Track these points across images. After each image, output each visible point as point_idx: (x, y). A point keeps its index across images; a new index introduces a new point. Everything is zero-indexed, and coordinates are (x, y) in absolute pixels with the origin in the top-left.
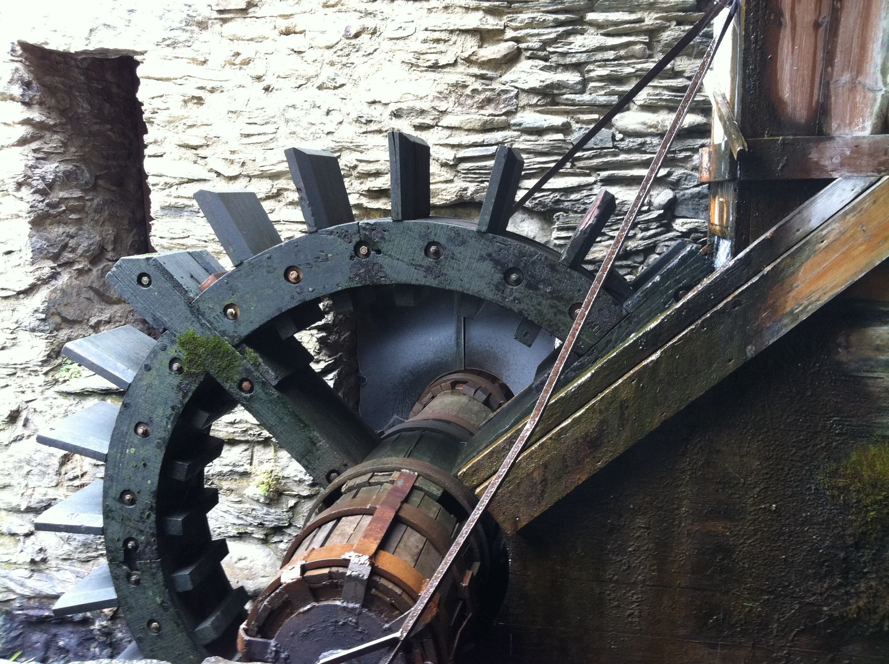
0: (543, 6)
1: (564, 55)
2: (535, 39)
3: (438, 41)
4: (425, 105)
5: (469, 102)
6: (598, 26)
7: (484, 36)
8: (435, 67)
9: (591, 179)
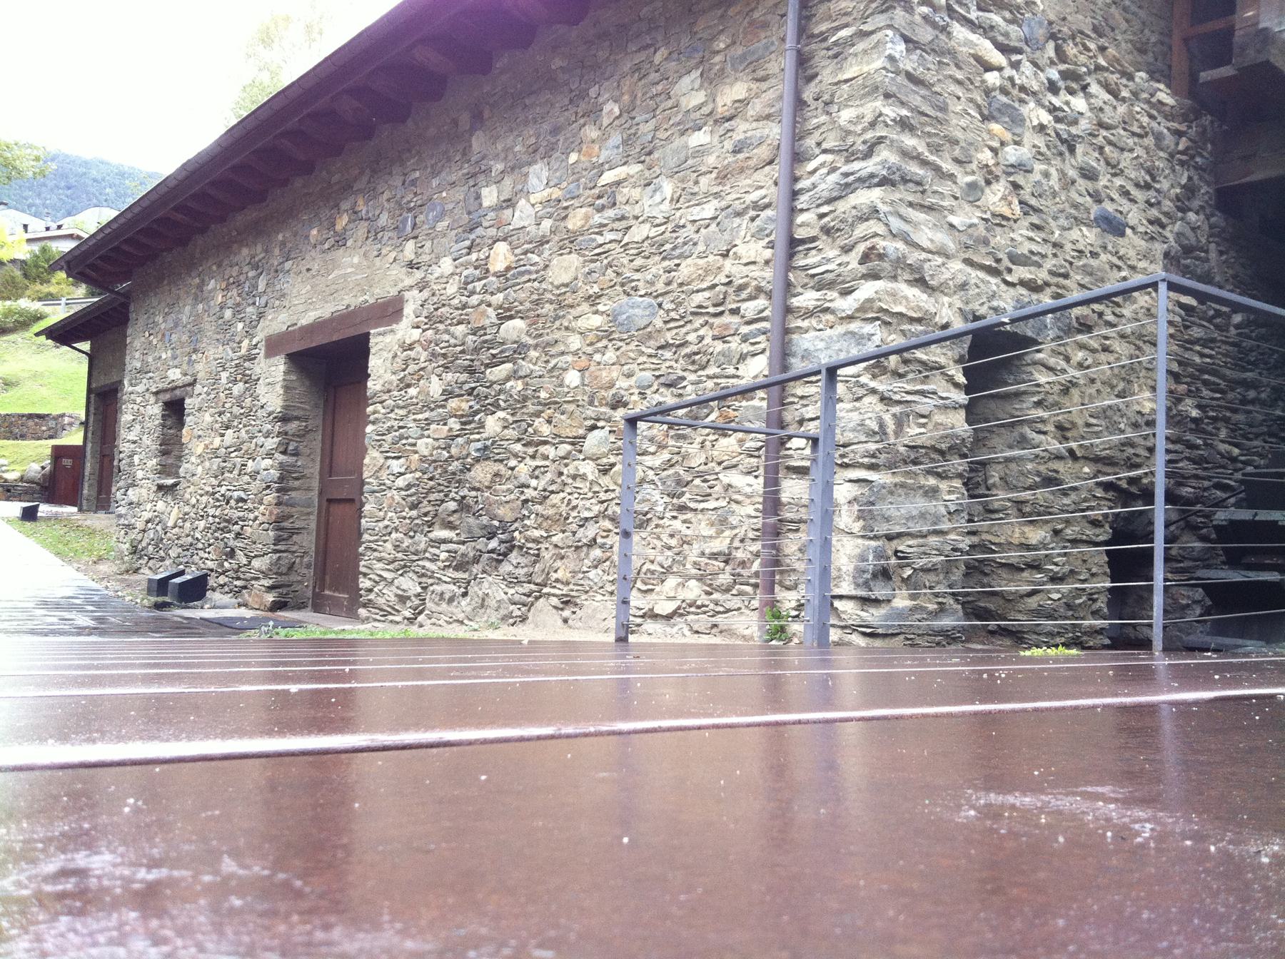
6: (1205, 383)
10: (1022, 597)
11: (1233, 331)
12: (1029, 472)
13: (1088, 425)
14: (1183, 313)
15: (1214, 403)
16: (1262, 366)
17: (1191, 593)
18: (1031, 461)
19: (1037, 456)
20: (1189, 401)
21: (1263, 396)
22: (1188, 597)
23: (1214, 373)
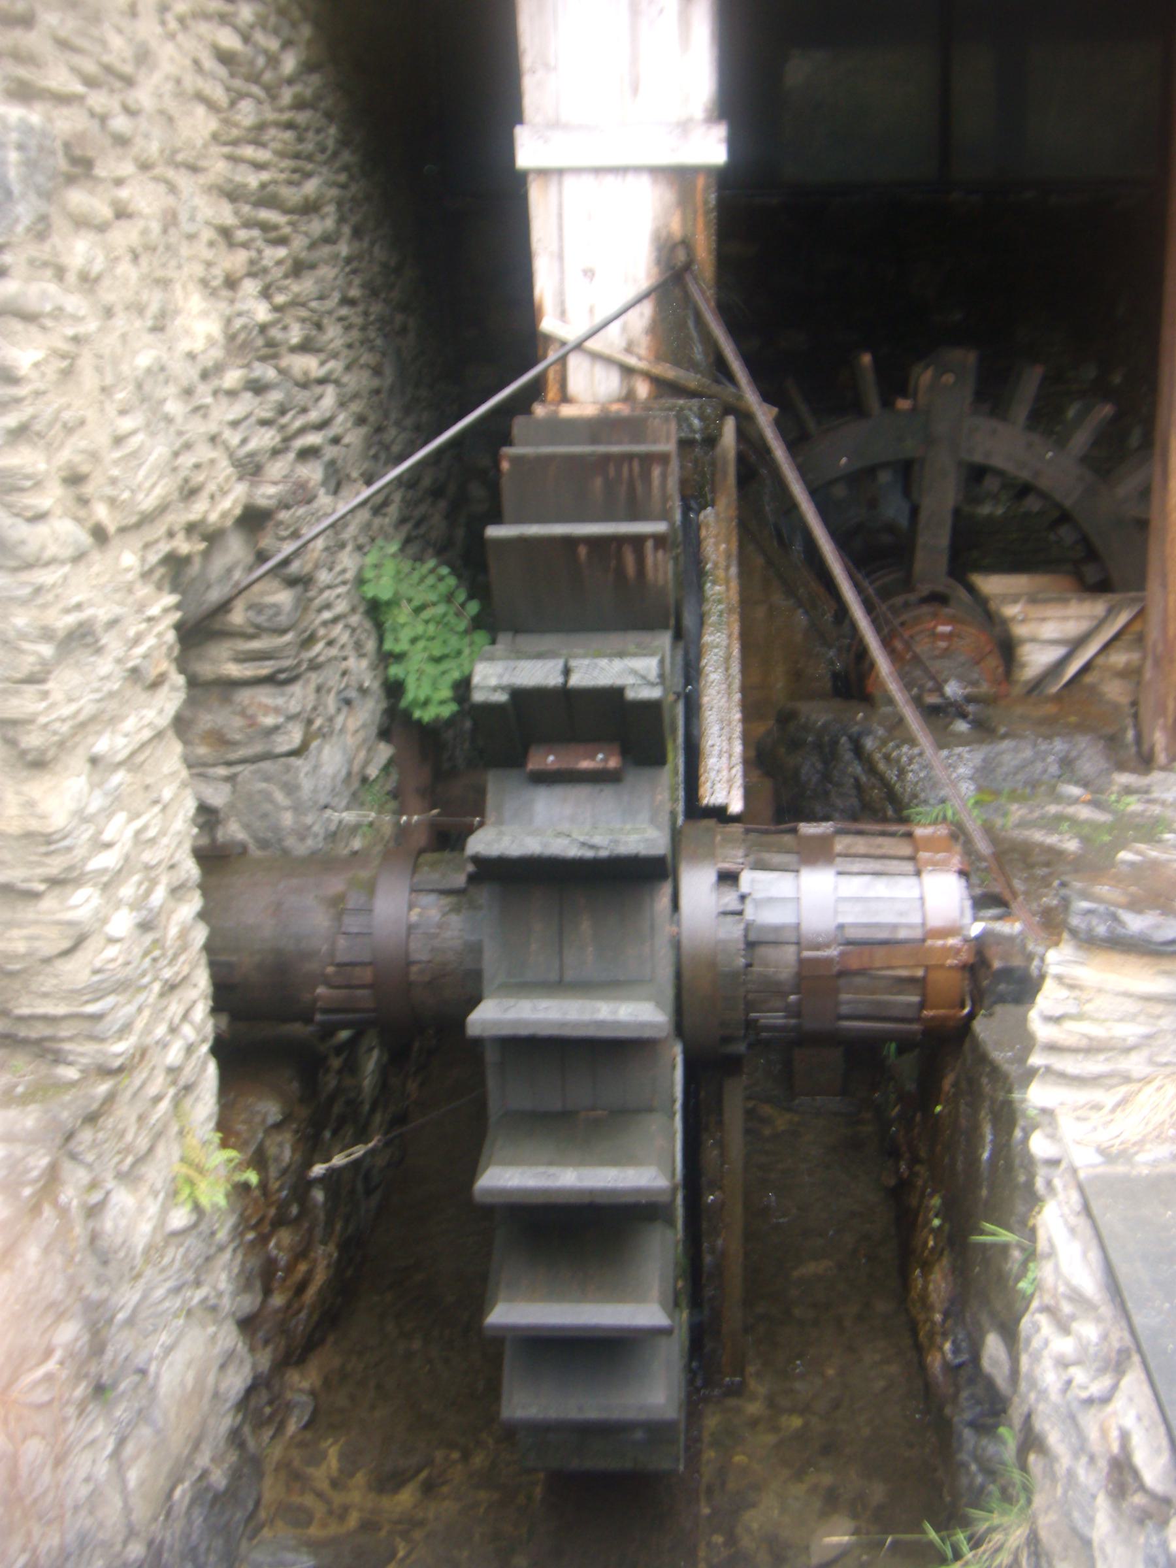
10: (47, 961)
12: (23, 636)
13: (118, 441)
17: (280, 701)
18: (25, 602)
19: (39, 590)
22: (277, 710)
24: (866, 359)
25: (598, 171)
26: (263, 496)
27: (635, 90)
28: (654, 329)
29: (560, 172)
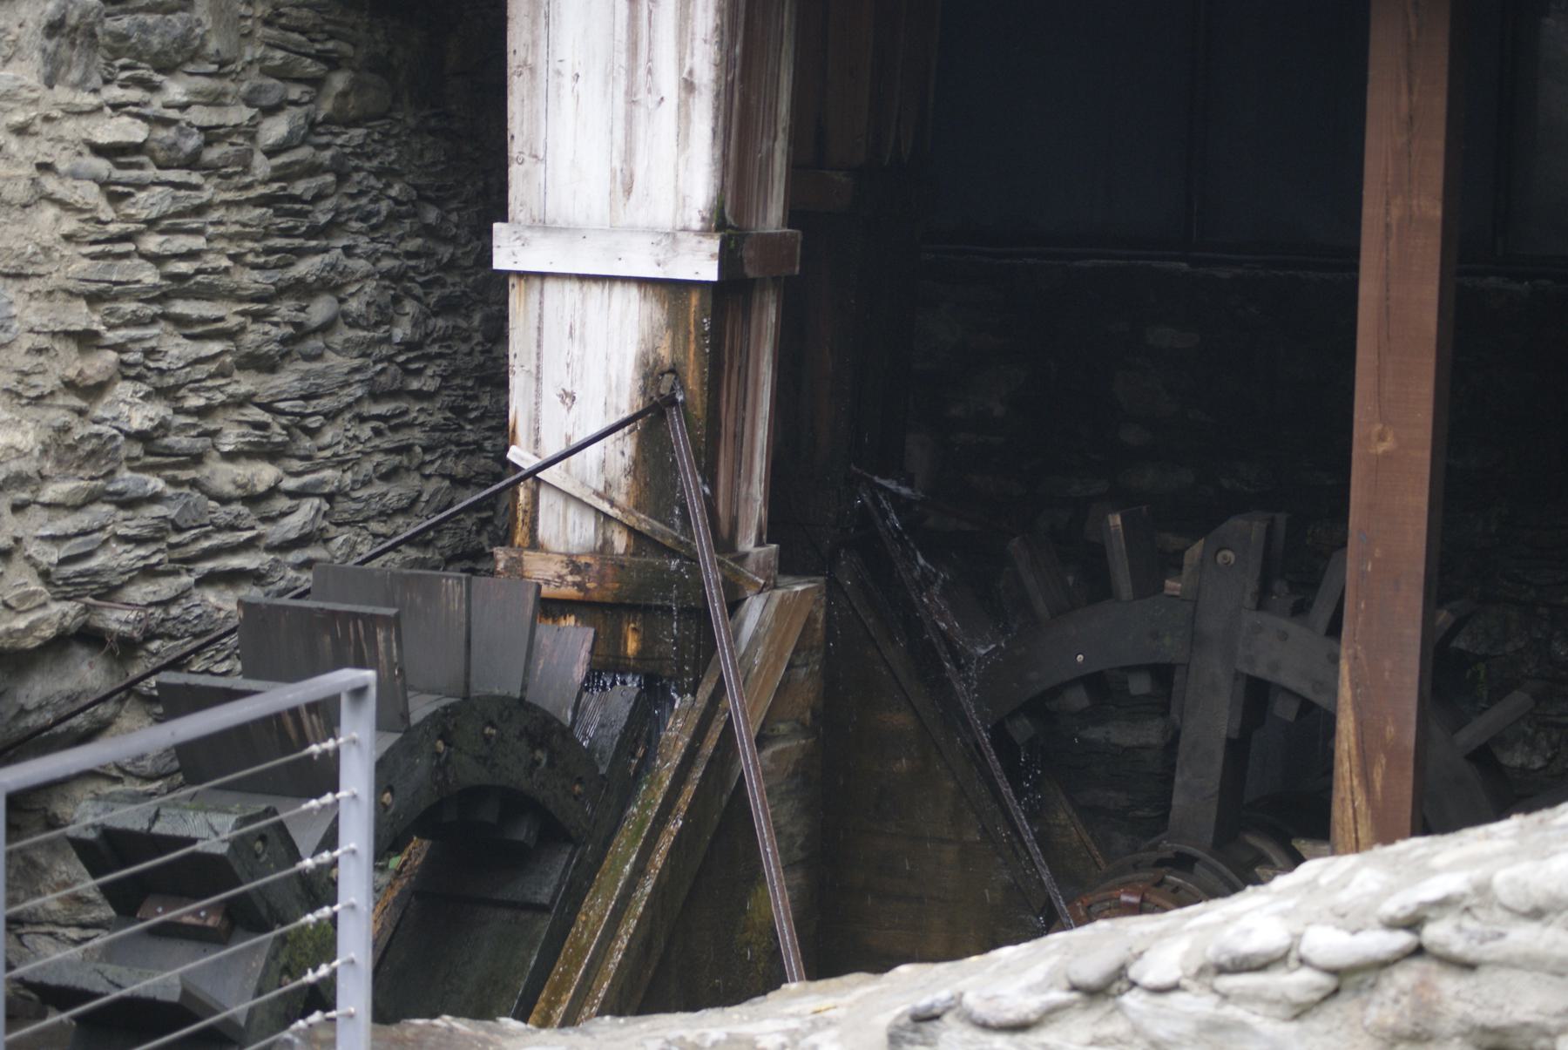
0: (146, 292)
1: (161, 372)
2: (137, 346)
3: (40, 351)
4: (28, 467)
5: (69, 456)
6: (180, 321)
7: (86, 340)
8: (38, 400)
9: (187, 579)
11: (262, 166)
14: (102, 166)
15: (201, 371)
16: (355, 225)
20: (124, 389)
21: (354, 305)
23: (208, 293)
24: (1116, 520)
25: (582, 278)
26: (118, 621)
27: (628, 190)
28: (635, 469)
29: (543, 276)
